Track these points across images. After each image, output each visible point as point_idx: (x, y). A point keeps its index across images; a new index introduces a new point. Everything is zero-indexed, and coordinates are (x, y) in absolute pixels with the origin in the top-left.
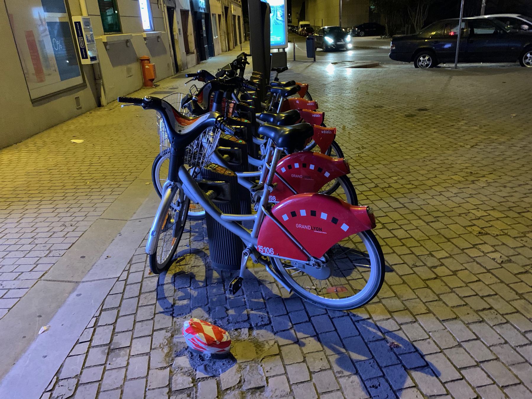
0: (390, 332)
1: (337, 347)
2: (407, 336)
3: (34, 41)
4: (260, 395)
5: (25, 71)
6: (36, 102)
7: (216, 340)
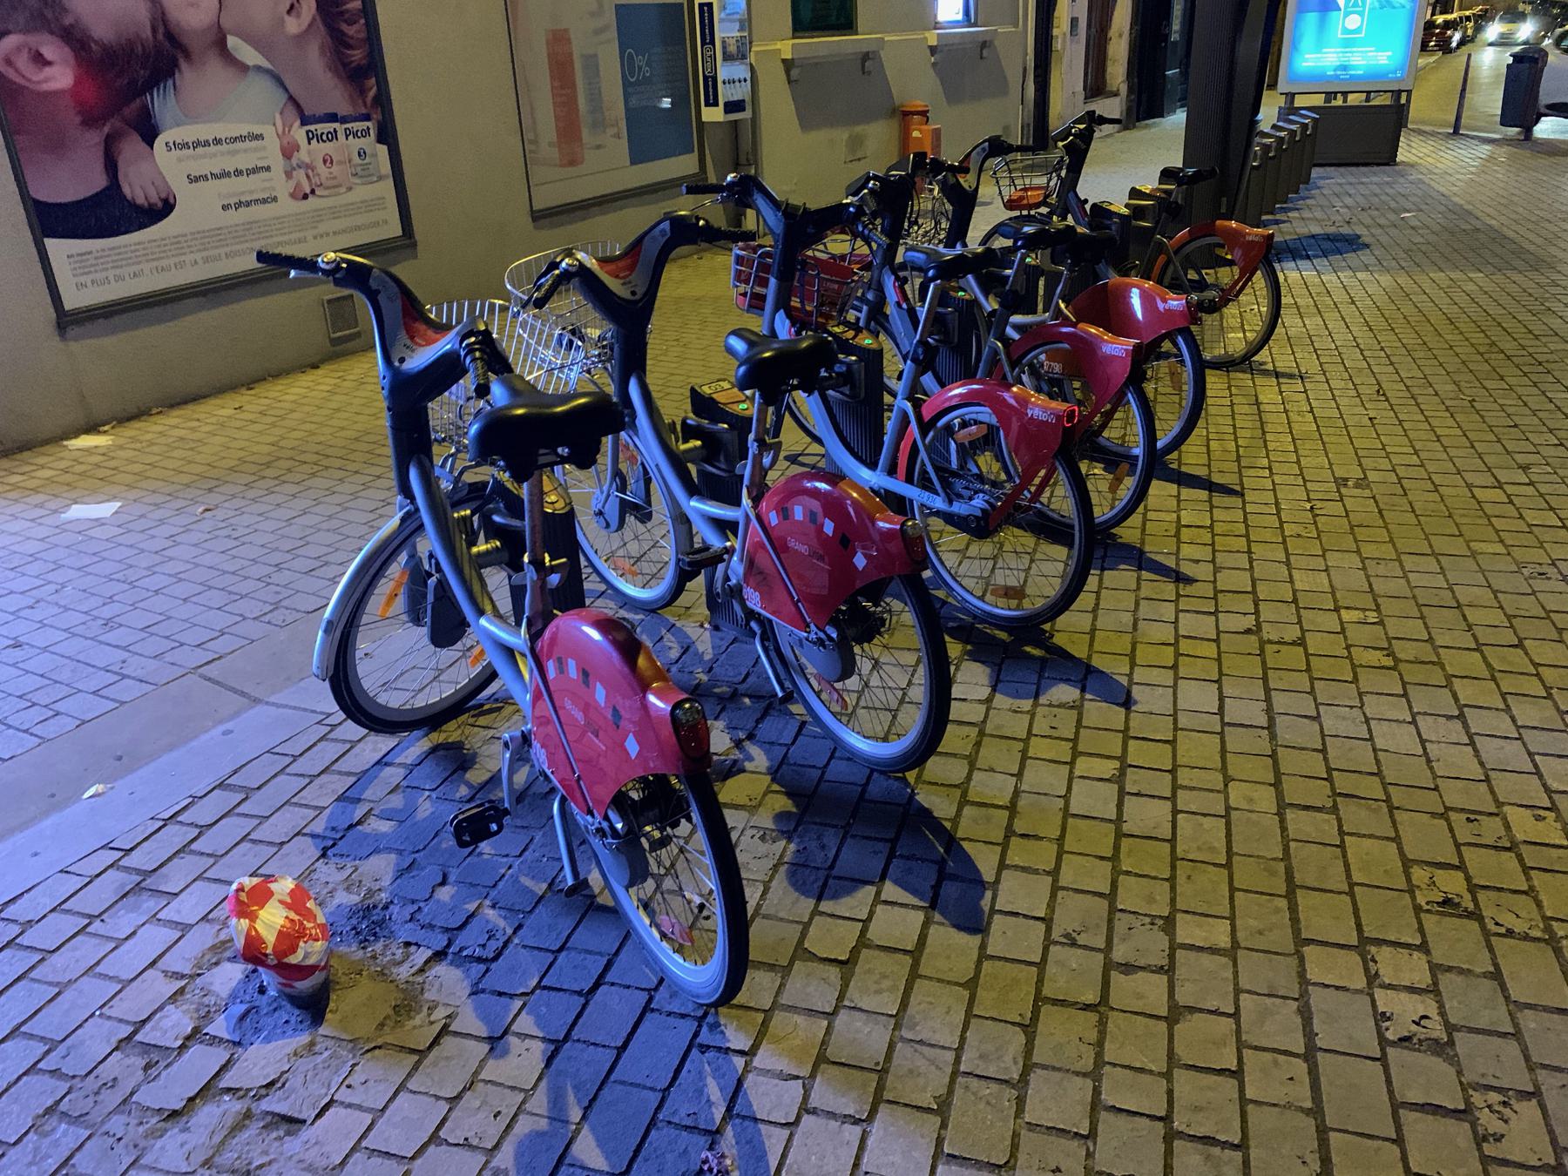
0: (756, 1120)
1: (571, 1098)
2: (784, 1156)
3: (571, 55)
4: (279, 1138)
5: (528, 136)
6: (541, 217)
7: (269, 951)
